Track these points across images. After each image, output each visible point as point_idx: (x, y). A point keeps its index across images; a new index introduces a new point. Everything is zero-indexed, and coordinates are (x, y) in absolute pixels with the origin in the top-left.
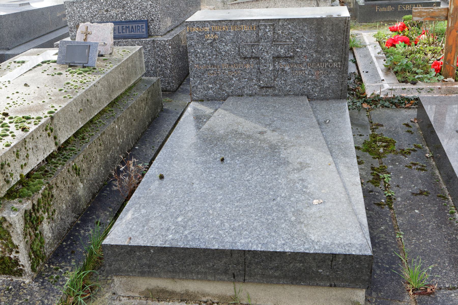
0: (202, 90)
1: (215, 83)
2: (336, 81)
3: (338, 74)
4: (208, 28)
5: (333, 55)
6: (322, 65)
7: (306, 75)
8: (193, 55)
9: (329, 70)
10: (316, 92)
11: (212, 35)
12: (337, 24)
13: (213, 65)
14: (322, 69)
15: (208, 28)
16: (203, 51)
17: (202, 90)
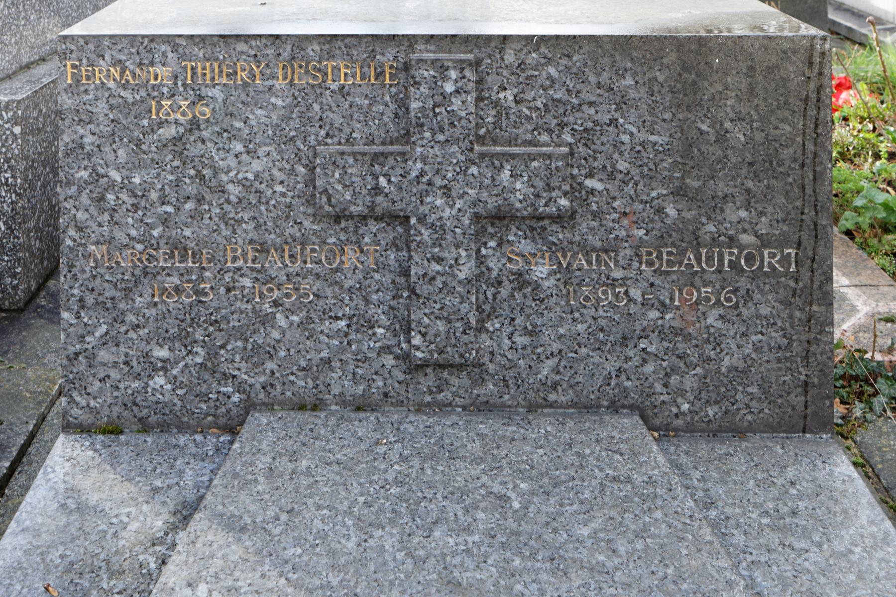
0: (115, 375)
1: (185, 340)
2: (776, 336)
3: (787, 304)
4: (164, 72)
5: (762, 214)
6: (710, 259)
7: (633, 309)
8: (84, 199)
9: (743, 283)
10: (682, 392)
11: (184, 104)
12: (770, 70)
13: (178, 248)
14: (707, 277)
15: (164, 72)
16: (137, 180)
17: (115, 375)
